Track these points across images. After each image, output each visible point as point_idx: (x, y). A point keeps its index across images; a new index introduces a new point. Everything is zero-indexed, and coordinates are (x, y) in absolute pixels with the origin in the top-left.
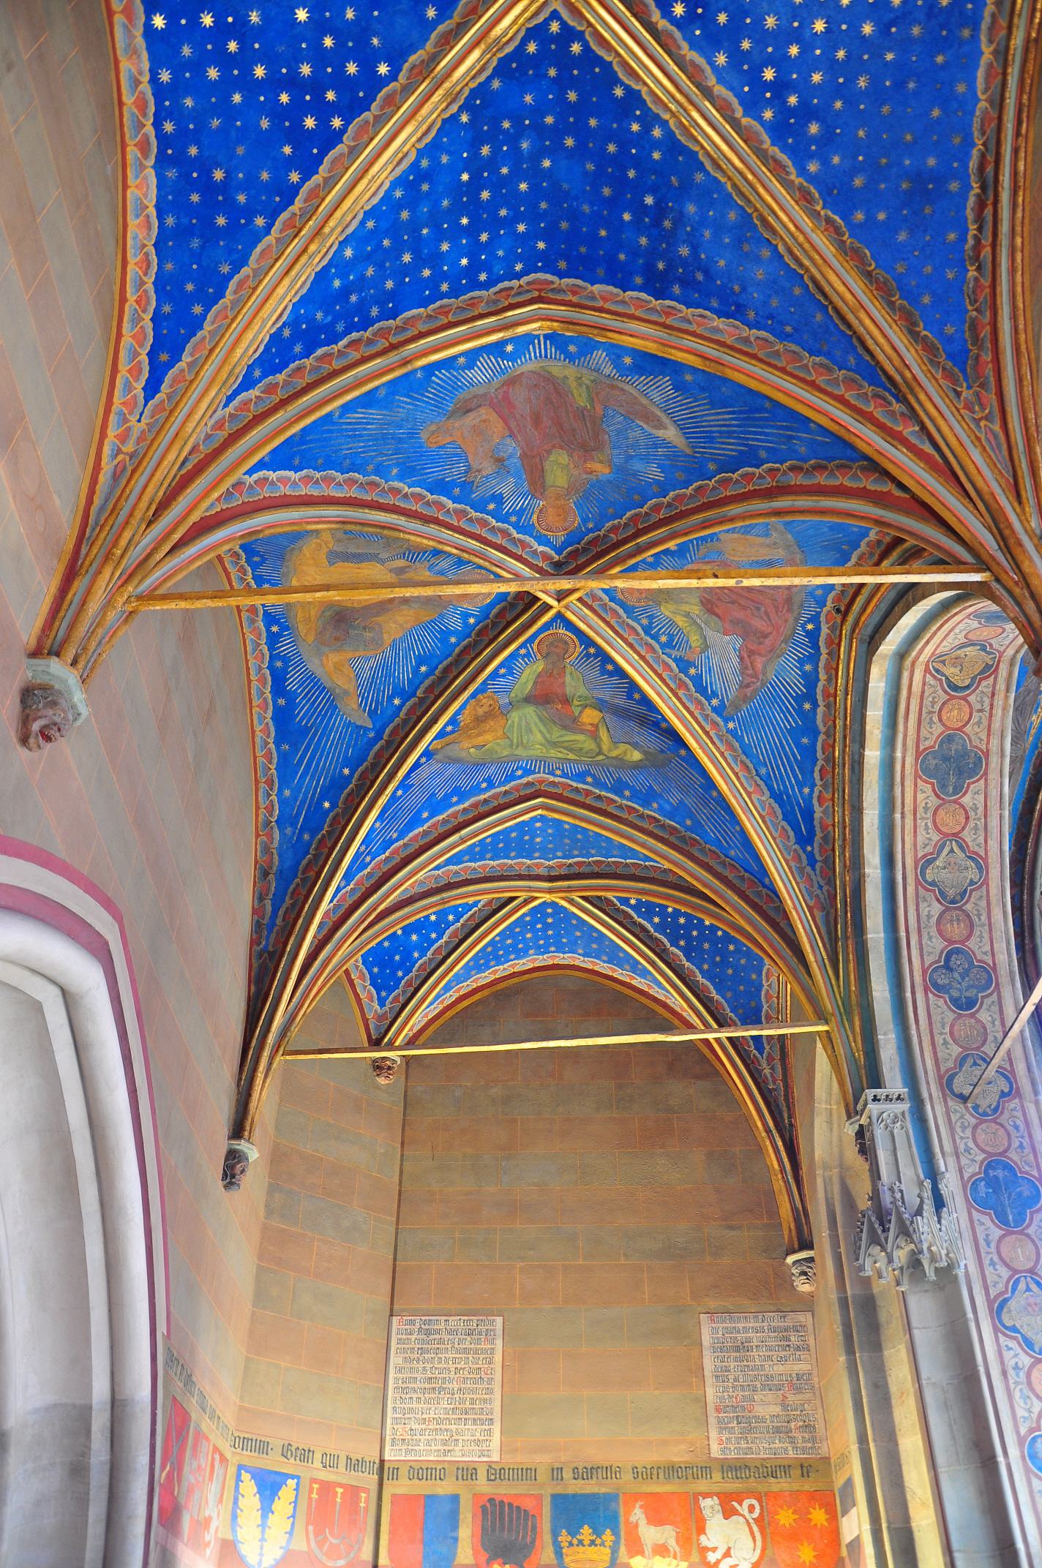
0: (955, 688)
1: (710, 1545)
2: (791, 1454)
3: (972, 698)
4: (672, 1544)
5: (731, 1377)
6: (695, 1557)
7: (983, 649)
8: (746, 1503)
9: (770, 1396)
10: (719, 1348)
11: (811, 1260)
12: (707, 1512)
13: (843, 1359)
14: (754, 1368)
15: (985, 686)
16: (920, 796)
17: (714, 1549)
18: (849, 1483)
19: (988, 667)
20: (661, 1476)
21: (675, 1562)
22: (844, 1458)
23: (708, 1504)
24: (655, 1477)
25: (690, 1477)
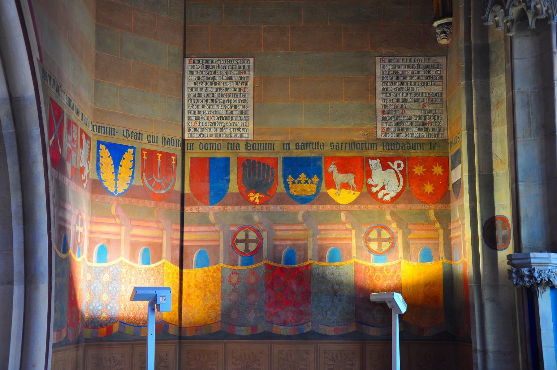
1: (373, 183)
2: (425, 137)
4: (352, 183)
5: (392, 94)
6: (365, 189)
8: (396, 163)
9: (415, 105)
10: (386, 77)
11: (449, 24)
13: (463, 83)
18: (459, 152)
21: (353, 192)
22: (458, 139)
23: (374, 164)
24: (343, 148)
25: (364, 148)
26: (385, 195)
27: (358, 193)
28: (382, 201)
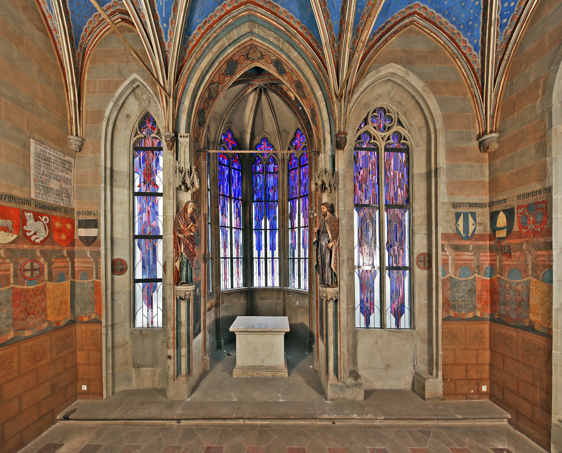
1: (28, 230)
2: (62, 205)
6: (21, 233)
8: (44, 217)
12: (27, 218)
14: (51, 170)
17: (30, 232)
20: (7, 199)
21: (11, 234)
25: (21, 203)
26: (36, 239)
27: (15, 236)
28: (34, 243)
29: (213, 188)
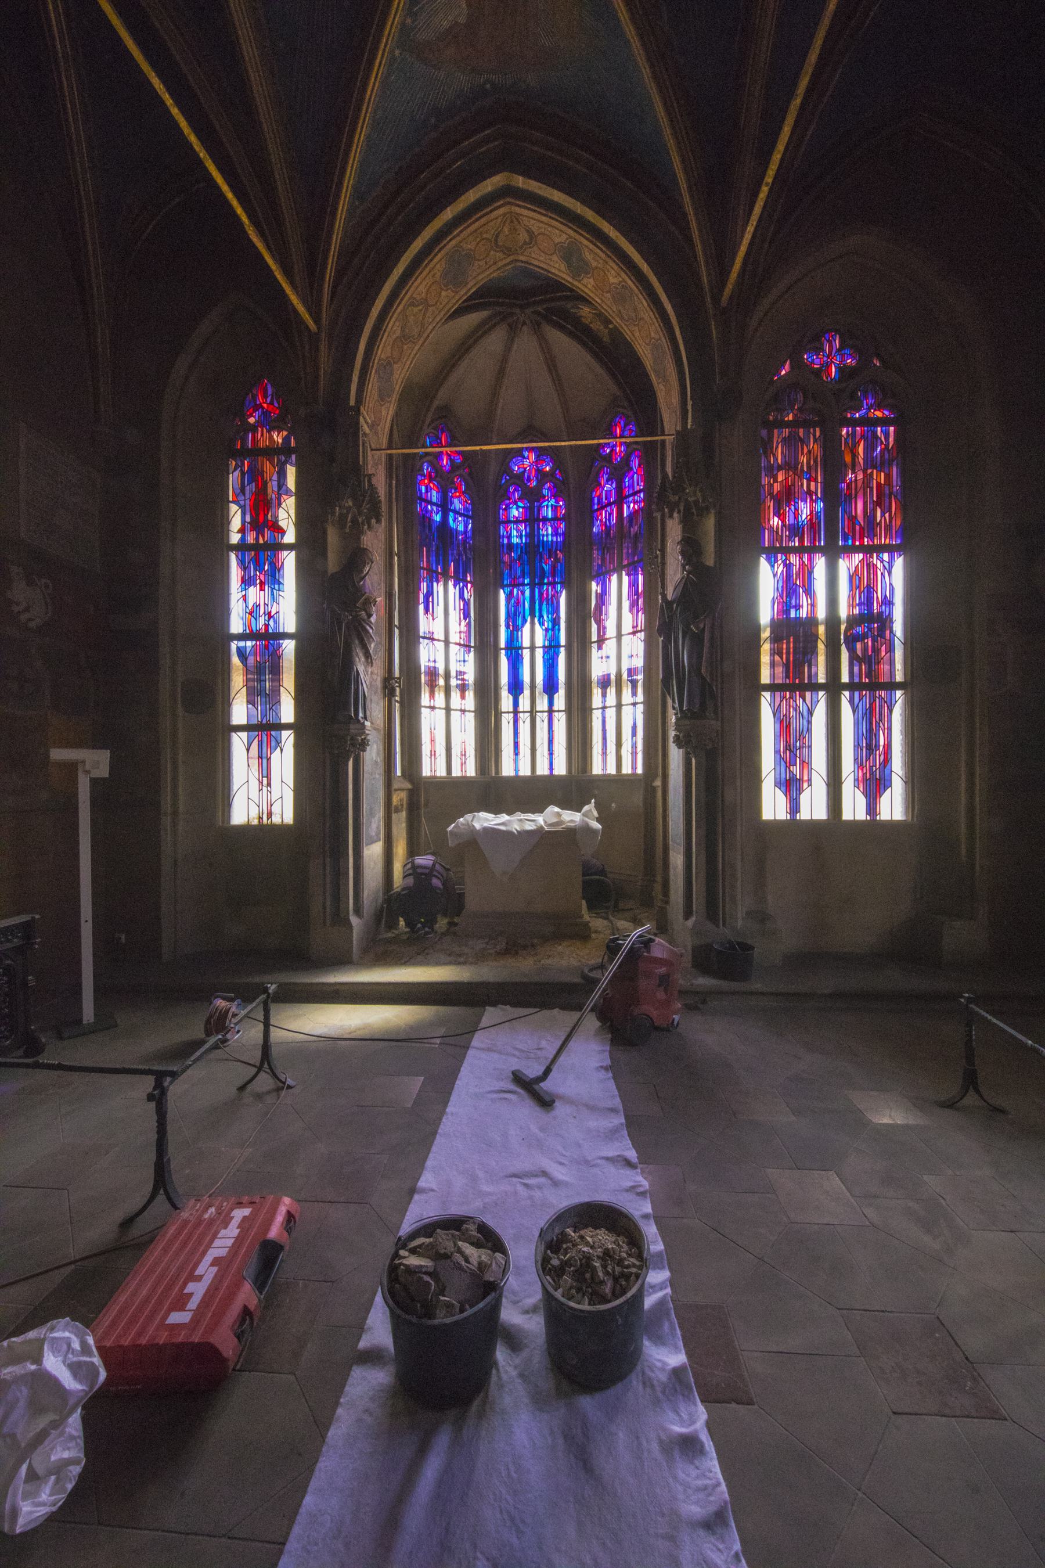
0: (496, 240)
3: (492, 253)
7: (525, 243)
8: (43, 581)
15: (500, 255)
16: (438, 266)
17: (17, 604)
19: (509, 249)
29: (402, 548)
